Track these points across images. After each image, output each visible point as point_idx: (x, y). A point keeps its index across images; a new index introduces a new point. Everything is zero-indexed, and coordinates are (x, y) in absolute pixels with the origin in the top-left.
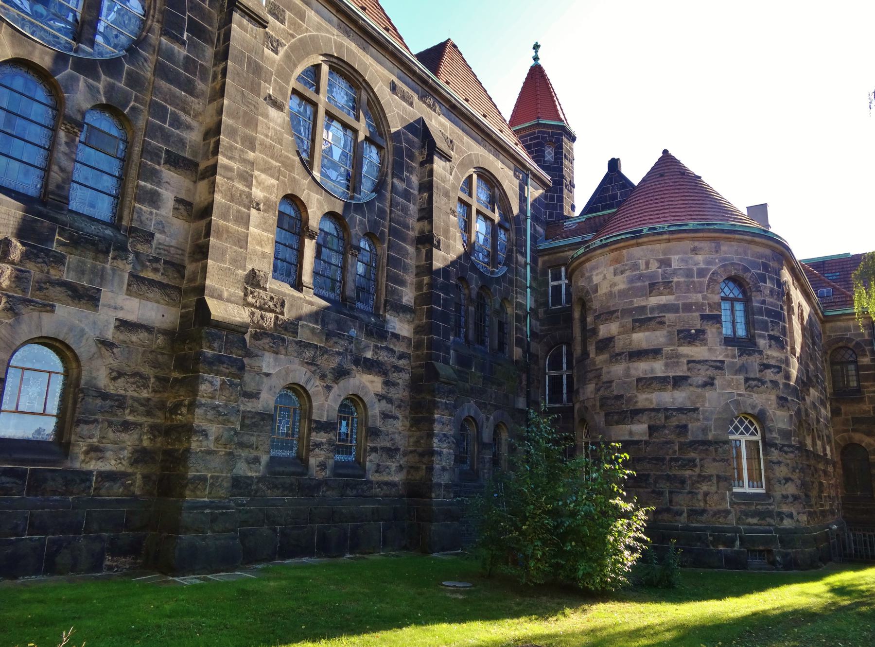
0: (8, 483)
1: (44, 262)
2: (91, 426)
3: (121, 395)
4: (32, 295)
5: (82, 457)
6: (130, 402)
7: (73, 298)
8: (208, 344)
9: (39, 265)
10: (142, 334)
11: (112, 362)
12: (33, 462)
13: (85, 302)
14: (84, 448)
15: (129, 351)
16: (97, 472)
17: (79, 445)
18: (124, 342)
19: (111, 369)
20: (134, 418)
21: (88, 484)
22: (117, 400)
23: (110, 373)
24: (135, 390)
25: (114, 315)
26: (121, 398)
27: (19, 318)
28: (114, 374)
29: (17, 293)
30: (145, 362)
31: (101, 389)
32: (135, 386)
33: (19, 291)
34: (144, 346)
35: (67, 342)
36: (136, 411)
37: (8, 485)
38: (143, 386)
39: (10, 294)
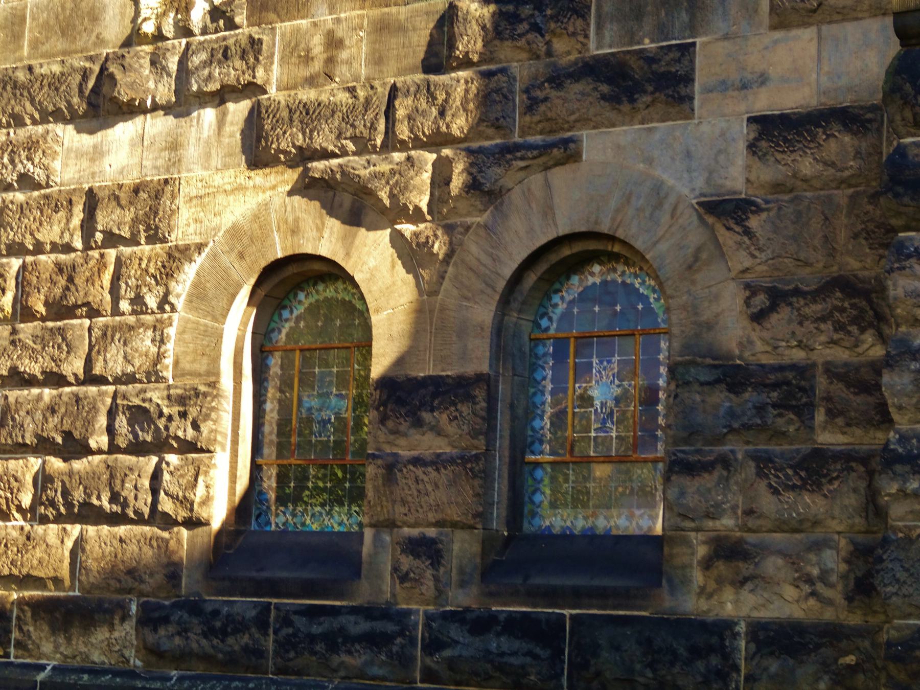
0: (514, 654)
1: (536, 28)
2: (708, 480)
3: (793, 367)
4: (523, 134)
5: (698, 577)
6: (822, 383)
7: (613, 100)
8: (908, 114)
9: (522, 42)
10: (833, 145)
11: (748, 262)
12: (576, 596)
13: (647, 99)
14: (702, 551)
15: (799, 214)
16: (749, 625)
17: (687, 542)
18: (778, 187)
19: (747, 286)
20: (841, 439)
21: (715, 660)
22: (775, 386)
23: (747, 302)
24: (833, 342)
25: (743, 107)
26: (790, 375)
27: (502, 204)
28: (761, 300)
29: (488, 138)
30: (856, 236)
31: (730, 357)
32: (827, 326)
33: (490, 131)
34: (843, 183)
35: (620, 234)
36: (841, 413)
37: (513, 660)
38: (854, 321)
39: (475, 145)
